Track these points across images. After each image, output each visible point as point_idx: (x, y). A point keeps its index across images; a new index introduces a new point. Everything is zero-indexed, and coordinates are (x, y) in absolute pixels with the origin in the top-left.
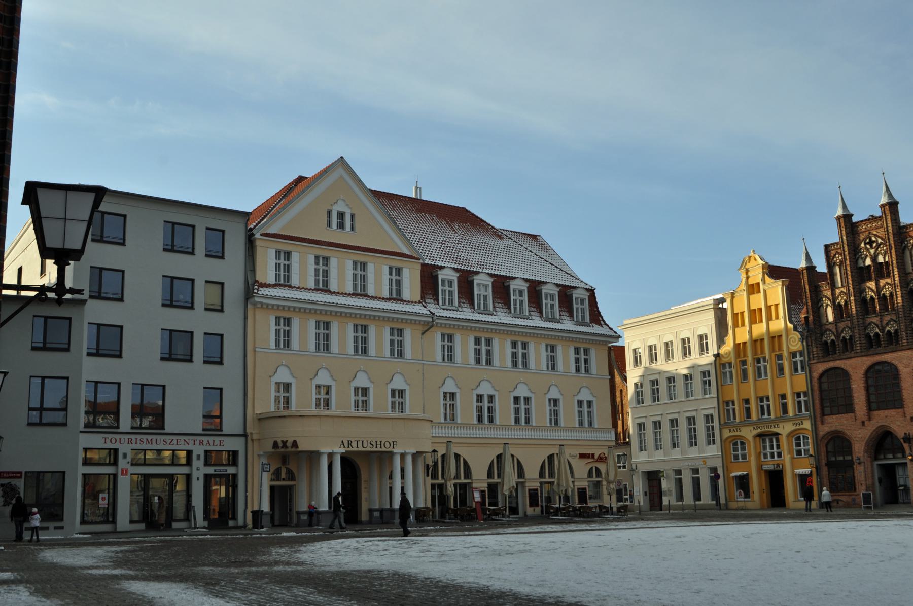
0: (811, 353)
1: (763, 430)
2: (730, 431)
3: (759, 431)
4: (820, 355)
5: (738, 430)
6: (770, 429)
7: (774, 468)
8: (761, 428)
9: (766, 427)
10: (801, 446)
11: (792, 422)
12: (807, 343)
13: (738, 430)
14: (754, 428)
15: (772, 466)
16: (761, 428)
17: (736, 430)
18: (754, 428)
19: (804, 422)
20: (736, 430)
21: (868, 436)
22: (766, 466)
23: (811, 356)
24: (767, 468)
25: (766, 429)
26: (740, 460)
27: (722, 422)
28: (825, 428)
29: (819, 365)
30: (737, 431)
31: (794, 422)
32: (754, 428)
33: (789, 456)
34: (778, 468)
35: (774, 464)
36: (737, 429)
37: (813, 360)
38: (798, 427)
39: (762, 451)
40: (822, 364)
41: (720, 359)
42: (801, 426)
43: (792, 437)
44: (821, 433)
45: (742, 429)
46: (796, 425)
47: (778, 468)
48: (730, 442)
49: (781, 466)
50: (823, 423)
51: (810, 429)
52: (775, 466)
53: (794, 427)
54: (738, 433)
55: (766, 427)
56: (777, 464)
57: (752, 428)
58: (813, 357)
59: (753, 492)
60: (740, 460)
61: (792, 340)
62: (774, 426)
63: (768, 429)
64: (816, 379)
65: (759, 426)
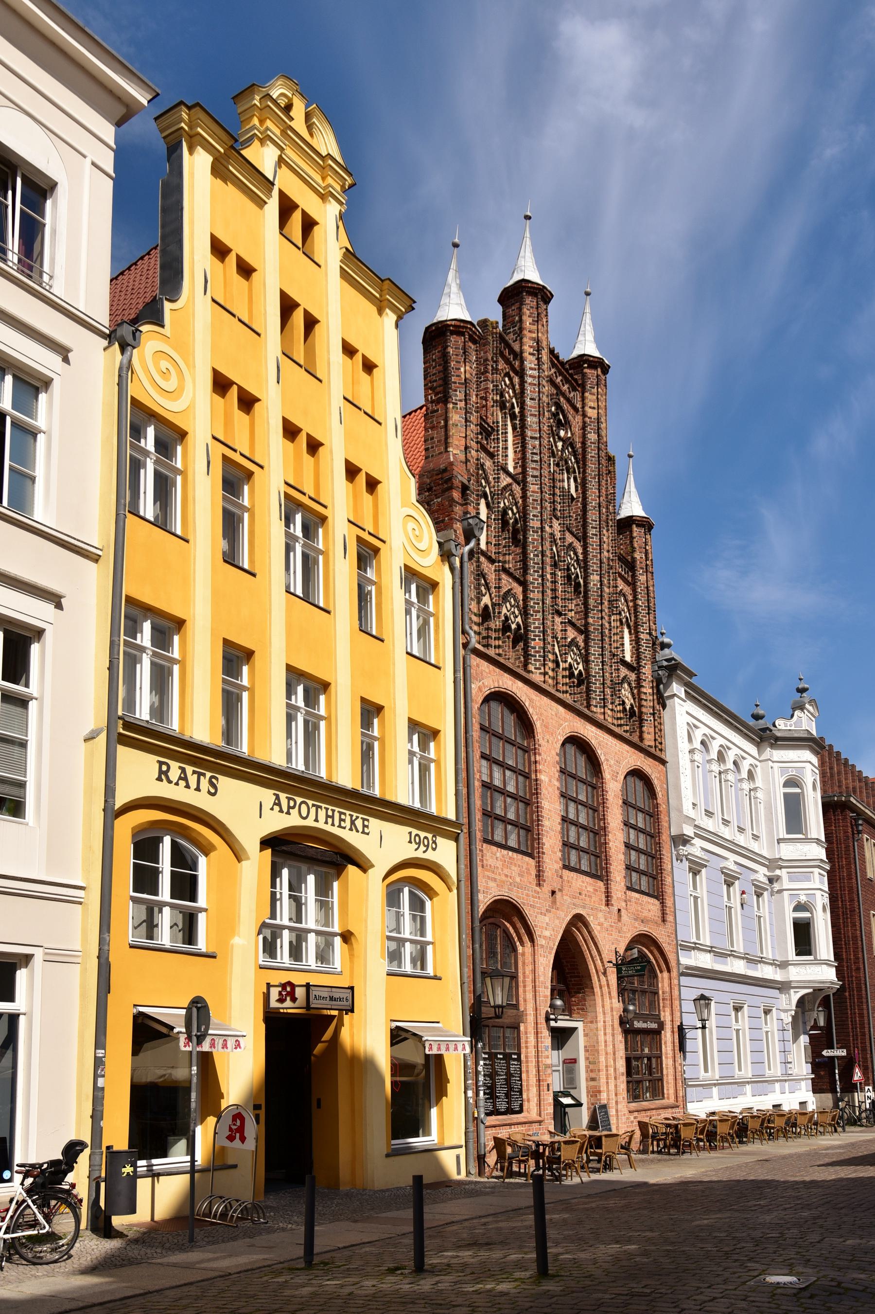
1: (310, 822)
2: (163, 775)
3: (293, 820)
5: (204, 783)
14: (278, 803)
17: (193, 780)
20: (193, 780)
21: (559, 938)
25: (321, 825)
30: (198, 789)
31: (415, 832)
32: (278, 803)
38: (420, 854)
42: (430, 855)
53: (410, 852)
54: (200, 800)
57: (267, 795)
63: (328, 828)
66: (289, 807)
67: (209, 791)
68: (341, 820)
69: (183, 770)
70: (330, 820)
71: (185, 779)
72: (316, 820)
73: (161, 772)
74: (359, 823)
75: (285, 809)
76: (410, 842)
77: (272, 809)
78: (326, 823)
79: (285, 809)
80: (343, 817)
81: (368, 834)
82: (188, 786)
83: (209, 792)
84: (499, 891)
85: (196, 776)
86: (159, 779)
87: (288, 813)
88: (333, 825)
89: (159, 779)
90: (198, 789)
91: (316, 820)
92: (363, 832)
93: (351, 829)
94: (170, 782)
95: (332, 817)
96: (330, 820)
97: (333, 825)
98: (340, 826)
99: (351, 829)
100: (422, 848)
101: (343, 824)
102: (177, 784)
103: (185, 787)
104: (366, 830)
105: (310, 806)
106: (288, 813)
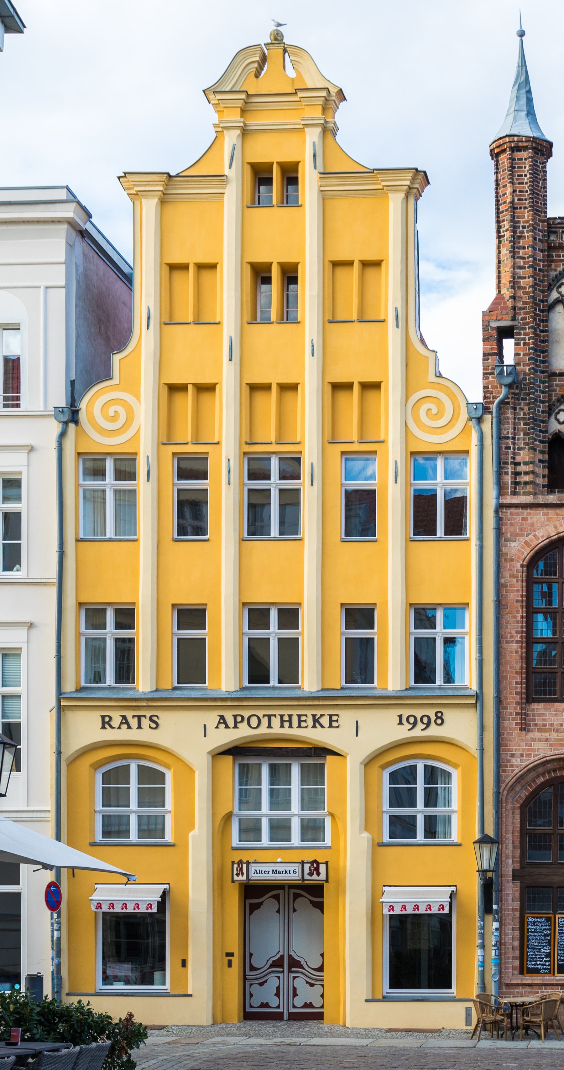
0: (510, 469)
1: (263, 730)
2: (106, 723)
4: (540, 481)
5: (146, 722)
6: (295, 732)
7: (303, 879)
8: (254, 722)
9: (276, 722)
10: (413, 805)
11: (399, 712)
12: (500, 422)
13: (146, 722)
15: (297, 868)
16: (254, 722)
17: (134, 723)
18: (222, 717)
19: (448, 714)
20: (134, 723)
22: (270, 868)
23: (508, 479)
24: (271, 876)
25: (276, 729)
26: (134, 837)
27: (69, 687)
28: (535, 745)
29: (539, 516)
30: (139, 727)
31: (406, 713)
33: (366, 835)
34: (315, 877)
35: (303, 863)
36: (139, 717)
37: (514, 493)
38: (418, 732)
39: (236, 810)
40: (551, 512)
41: (81, 433)
42: (434, 731)
43: (384, 767)
44: (516, 761)
45: (165, 717)
46: (415, 724)
47: (315, 877)
48: (96, 766)
49: (322, 868)
50: (524, 727)
51: (472, 743)
52: (307, 866)
53: (403, 732)
55: (276, 722)
56: (312, 863)
57: (212, 718)
58: (516, 483)
59: (184, 963)
60: (134, 837)
61: (424, 407)
62: (316, 721)
63: (286, 731)
64: (518, 565)
65: (246, 714)
66: (236, 723)
67: (150, 727)
68: (300, 721)
69: (124, 717)
70: (286, 724)
71: (127, 723)
72: (269, 726)
73: (103, 723)
74: (325, 721)
75: (231, 724)
76: (401, 723)
77: (217, 727)
78: (282, 726)
79: (231, 724)
80: (303, 718)
81: (338, 727)
82: (129, 727)
83: (150, 727)
84: (554, 750)
85: (136, 719)
86: (103, 727)
87: (235, 727)
88: (290, 726)
89: (103, 727)
90: (139, 727)
91: (269, 726)
92: (331, 726)
93: (314, 726)
94: (111, 727)
95: (290, 721)
96: (286, 724)
97: (290, 726)
98: (299, 726)
99: (314, 726)
100: (420, 726)
101: (303, 724)
102: (119, 728)
103: (128, 728)
104: (335, 724)
105: (261, 717)
106: (235, 727)
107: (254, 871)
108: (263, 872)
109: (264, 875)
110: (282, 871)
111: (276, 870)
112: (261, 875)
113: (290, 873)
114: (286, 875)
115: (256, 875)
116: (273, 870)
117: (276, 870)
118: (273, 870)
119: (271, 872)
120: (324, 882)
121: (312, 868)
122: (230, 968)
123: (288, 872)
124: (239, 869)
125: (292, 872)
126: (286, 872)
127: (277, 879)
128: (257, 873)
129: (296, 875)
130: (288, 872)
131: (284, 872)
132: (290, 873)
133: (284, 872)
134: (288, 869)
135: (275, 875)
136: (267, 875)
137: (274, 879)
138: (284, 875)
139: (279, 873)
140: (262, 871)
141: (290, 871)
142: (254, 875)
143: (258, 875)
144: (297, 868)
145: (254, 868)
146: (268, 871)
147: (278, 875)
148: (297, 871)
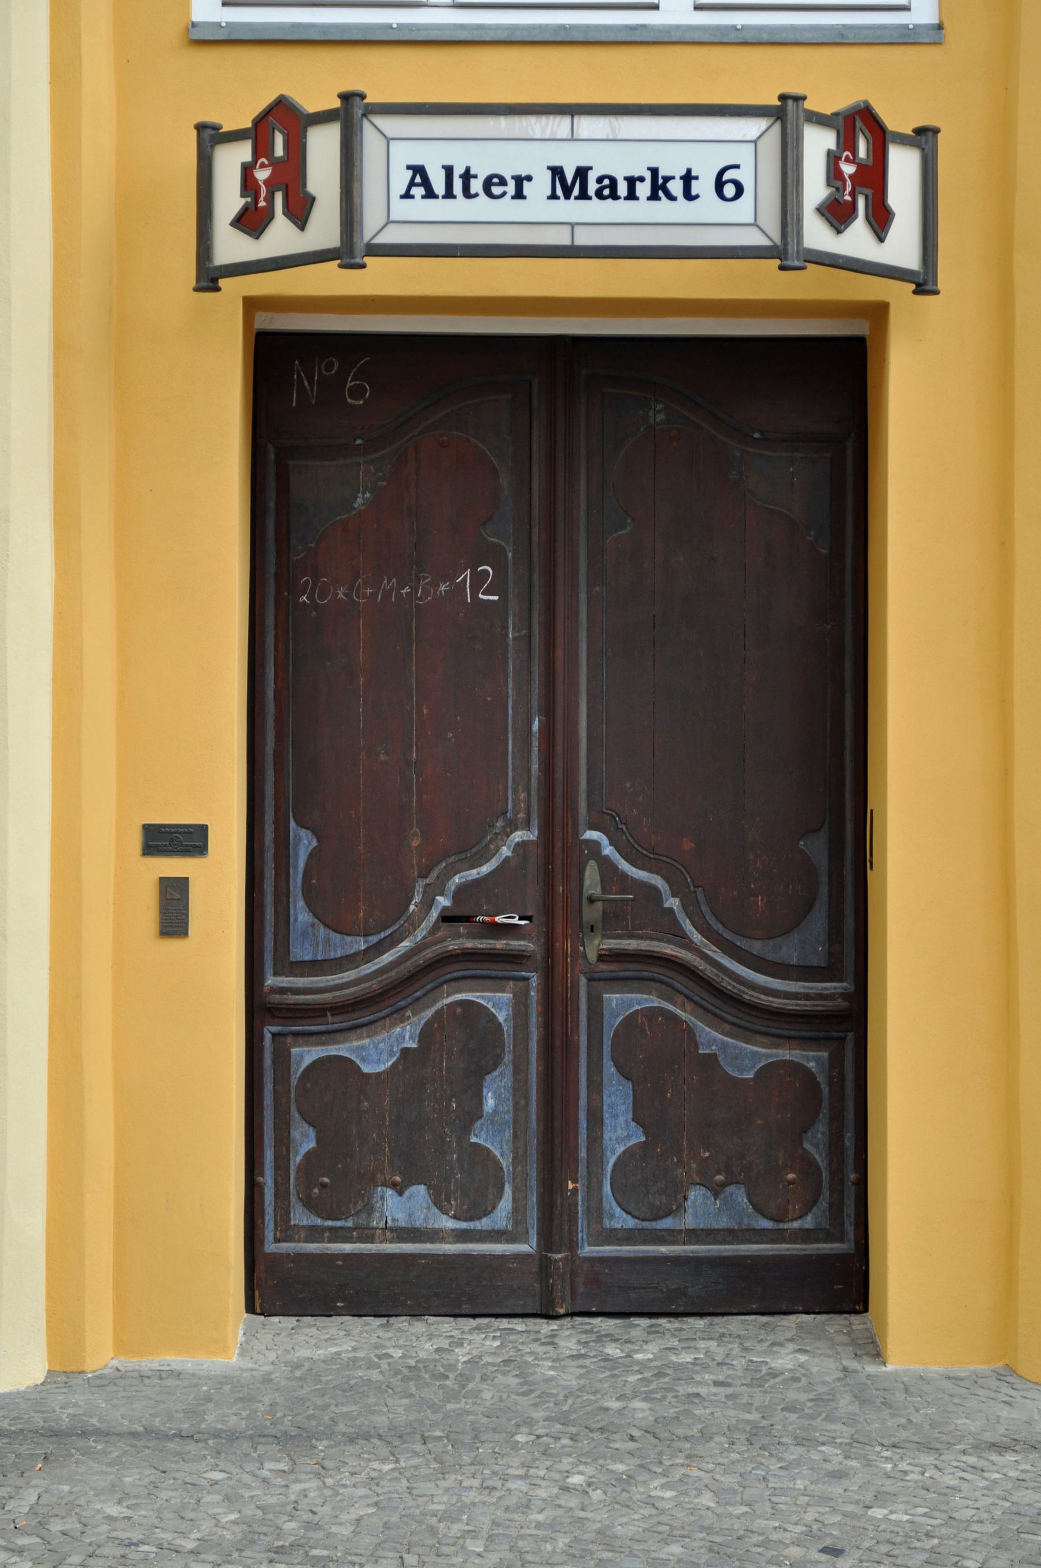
107: (401, 179)
108: (476, 186)
109: (482, 208)
110: (631, 181)
111: (582, 173)
112: (459, 208)
113: (688, 196)
114: (662, 210)
115: (420, 208)
116: (557, 172)
117: (582, 173)
118: (557, 172)
119: (540, 186)
120: (898, 293)
121: (848, 169)
122: (174, 945)
123: (676, 187)
124: (262, 175)
125: (704, 186)
126: (659, 188)
127: (585, 238)
128: (430, 194)
129: (742, 210)
130: (676, 187)
131: (643, 189)
132: (688, 196)
133: (643, 189)
134: (672, 167)
135: (571, 209)
136: (506, 209)
137: (560, 238)
138: (643, 209)
139: (608, 189)
140: (467, 176)
141: (688, 178)
142: (402, 209)
143: (439, 209)
144: (744, 156)
145: (404, 155)
146: (519, 181)
147: (595, 209)
148: (744, 176)
